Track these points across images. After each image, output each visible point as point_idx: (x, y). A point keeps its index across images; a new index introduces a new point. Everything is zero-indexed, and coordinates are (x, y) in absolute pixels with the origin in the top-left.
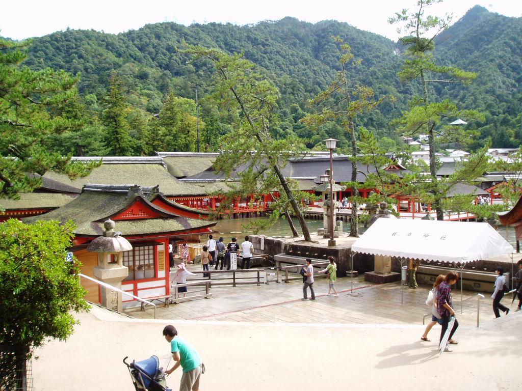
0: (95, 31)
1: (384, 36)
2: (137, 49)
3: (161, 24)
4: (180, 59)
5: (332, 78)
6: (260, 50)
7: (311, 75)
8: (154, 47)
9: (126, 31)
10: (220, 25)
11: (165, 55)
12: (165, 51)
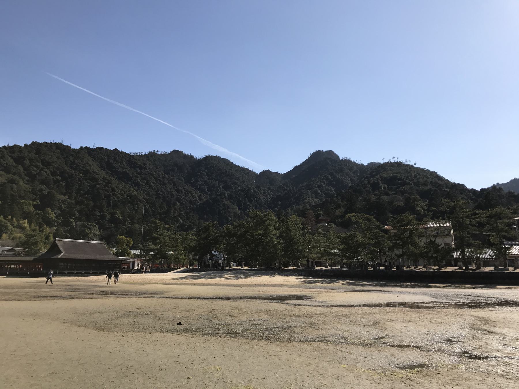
1: (250, 169)
2: (12, 161)
4: (51, 171)
5: (193, 196)
6: (137, 171)
7: (175, 193)
8: (31, 160)
9: (11, 145)
10: (107, 149)
11: (37, 167)
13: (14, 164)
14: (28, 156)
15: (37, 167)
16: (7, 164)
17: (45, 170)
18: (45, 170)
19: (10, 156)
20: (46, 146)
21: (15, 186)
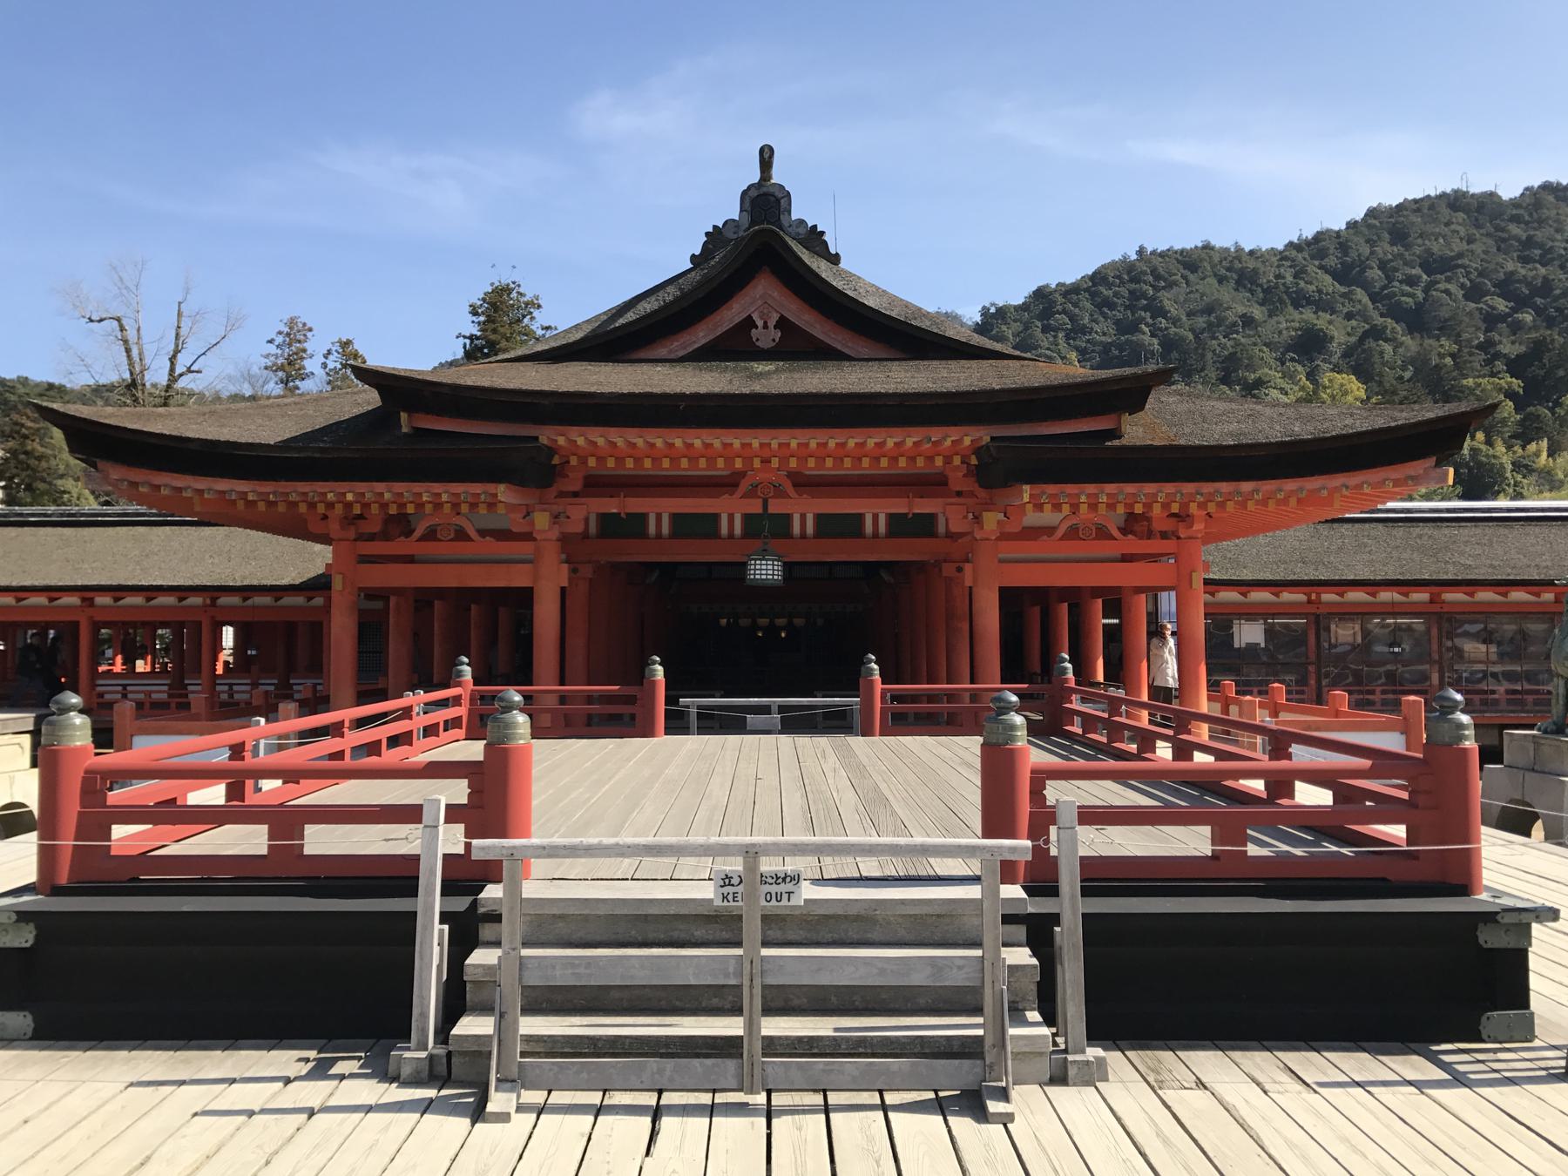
0: (1212, 248)
2: (1328, 279)
3: (1415, 201)
4: (1462, 286)
8: (1383, 266)
9: (1309, 234)
12: (1417, 271)
13: (1343, 289)
14: (1372, 253)
15: (1411, 281)
16: (1320, 291)
17: (1442, 286)
18: (1442, 286)
19: (1321, 267)
20: (1418, 210)
21: (1388, 348)
